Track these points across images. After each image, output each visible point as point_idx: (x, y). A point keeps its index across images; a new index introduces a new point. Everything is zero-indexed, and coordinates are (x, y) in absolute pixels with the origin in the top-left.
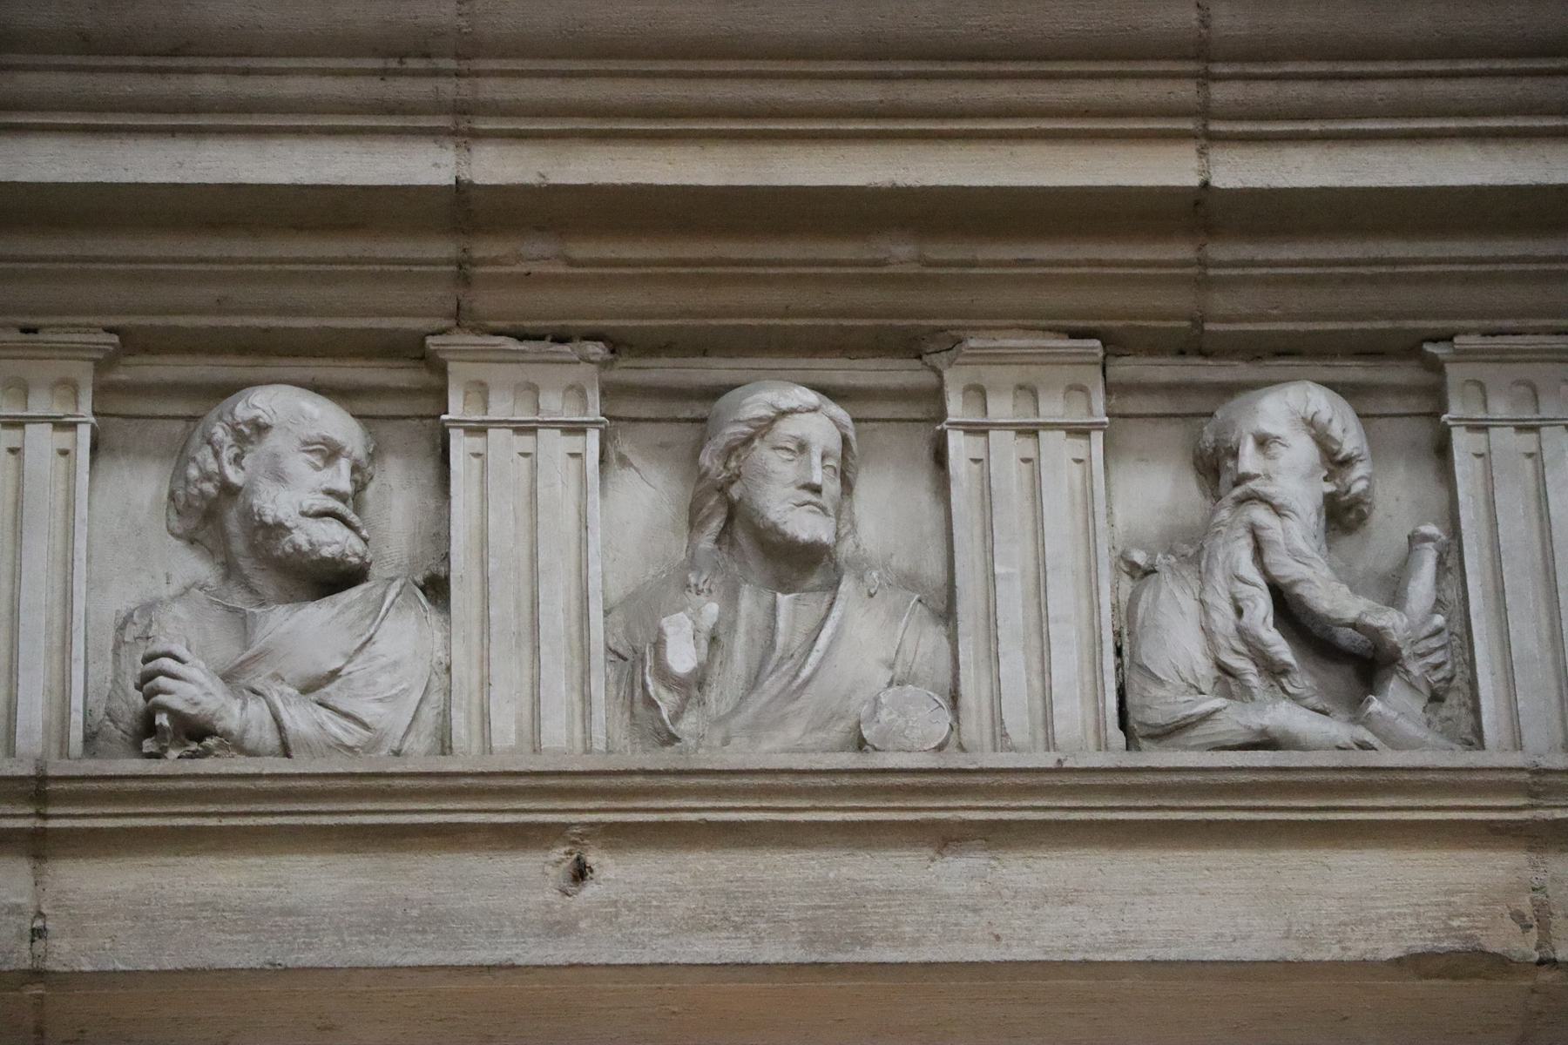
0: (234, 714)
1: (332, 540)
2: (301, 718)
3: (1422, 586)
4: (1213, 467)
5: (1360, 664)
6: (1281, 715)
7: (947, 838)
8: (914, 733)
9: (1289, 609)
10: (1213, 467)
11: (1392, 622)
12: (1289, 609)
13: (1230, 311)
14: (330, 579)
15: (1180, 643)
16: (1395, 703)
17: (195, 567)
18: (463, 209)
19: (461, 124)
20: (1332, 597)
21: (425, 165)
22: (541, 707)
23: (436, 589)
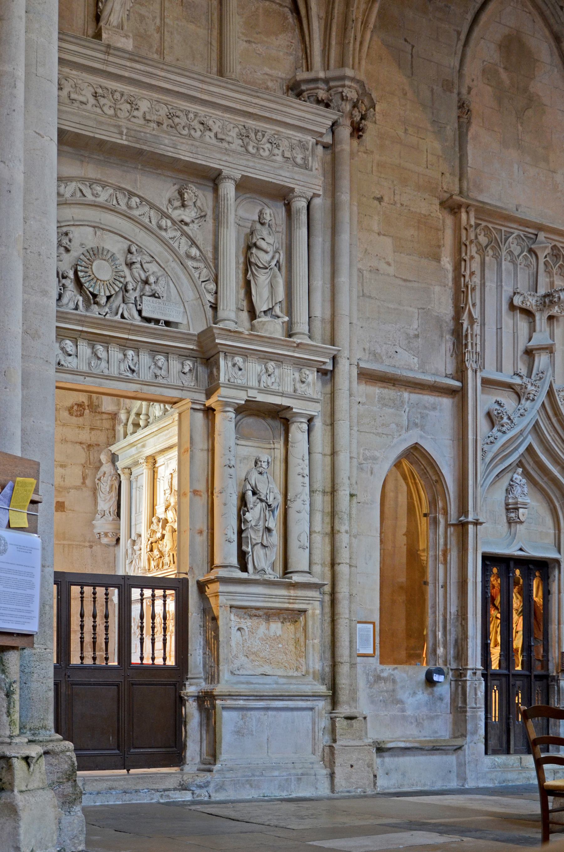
0: (65, 364)
1: (71, 353)
2: (69, 365)
3: (137, 366)
4: (125, 355)
5: (133, 371)
6: (129, 374)
7: (107, 379)
8: (106, 372)
9: (129, 367)
10: (125, 355)
11: (135, 369)
12: (129, 367)
13: (127, 345)
14: (70, 355)
15: (122, 368)
16: (135, 374)
17: (61, 352)
18: (81, 331)
19: (83, 326)
20: (132, 367)
21: (80, 328)
22: (84, 368)
23: (77, 356)
